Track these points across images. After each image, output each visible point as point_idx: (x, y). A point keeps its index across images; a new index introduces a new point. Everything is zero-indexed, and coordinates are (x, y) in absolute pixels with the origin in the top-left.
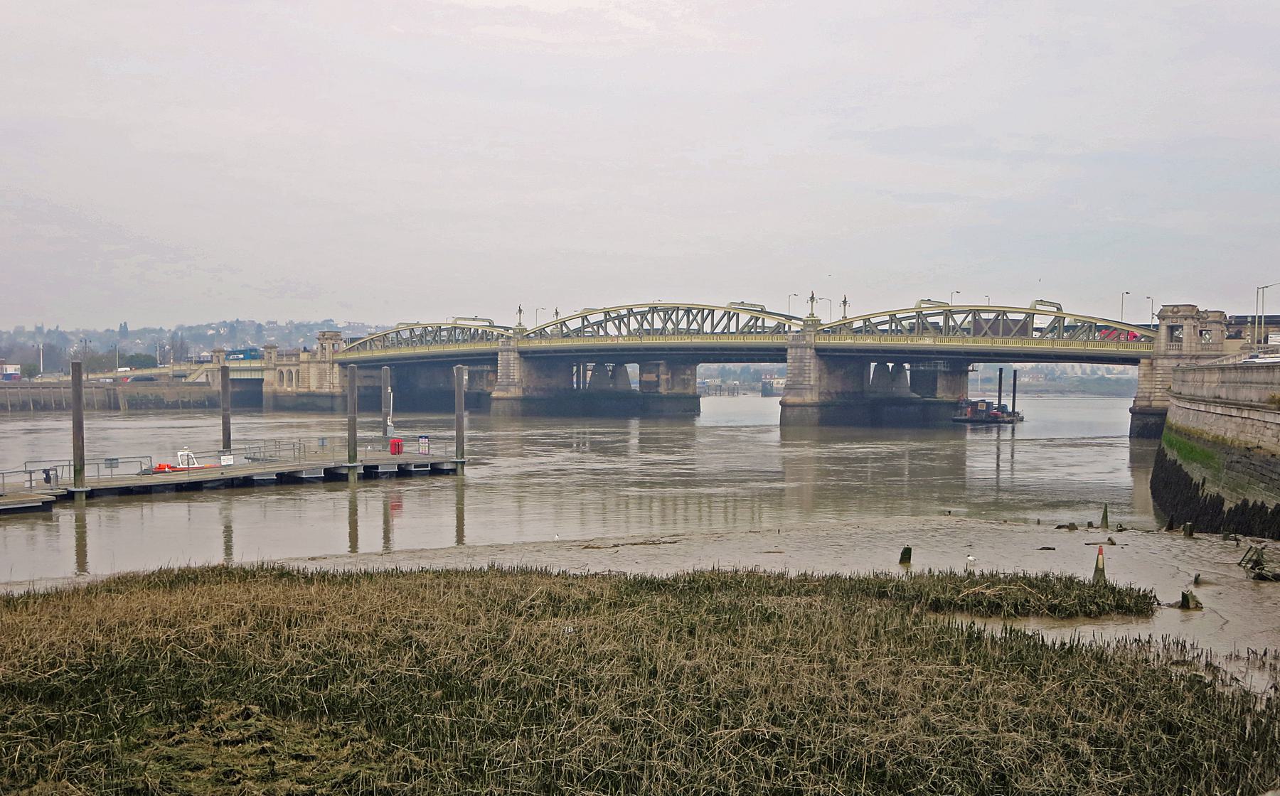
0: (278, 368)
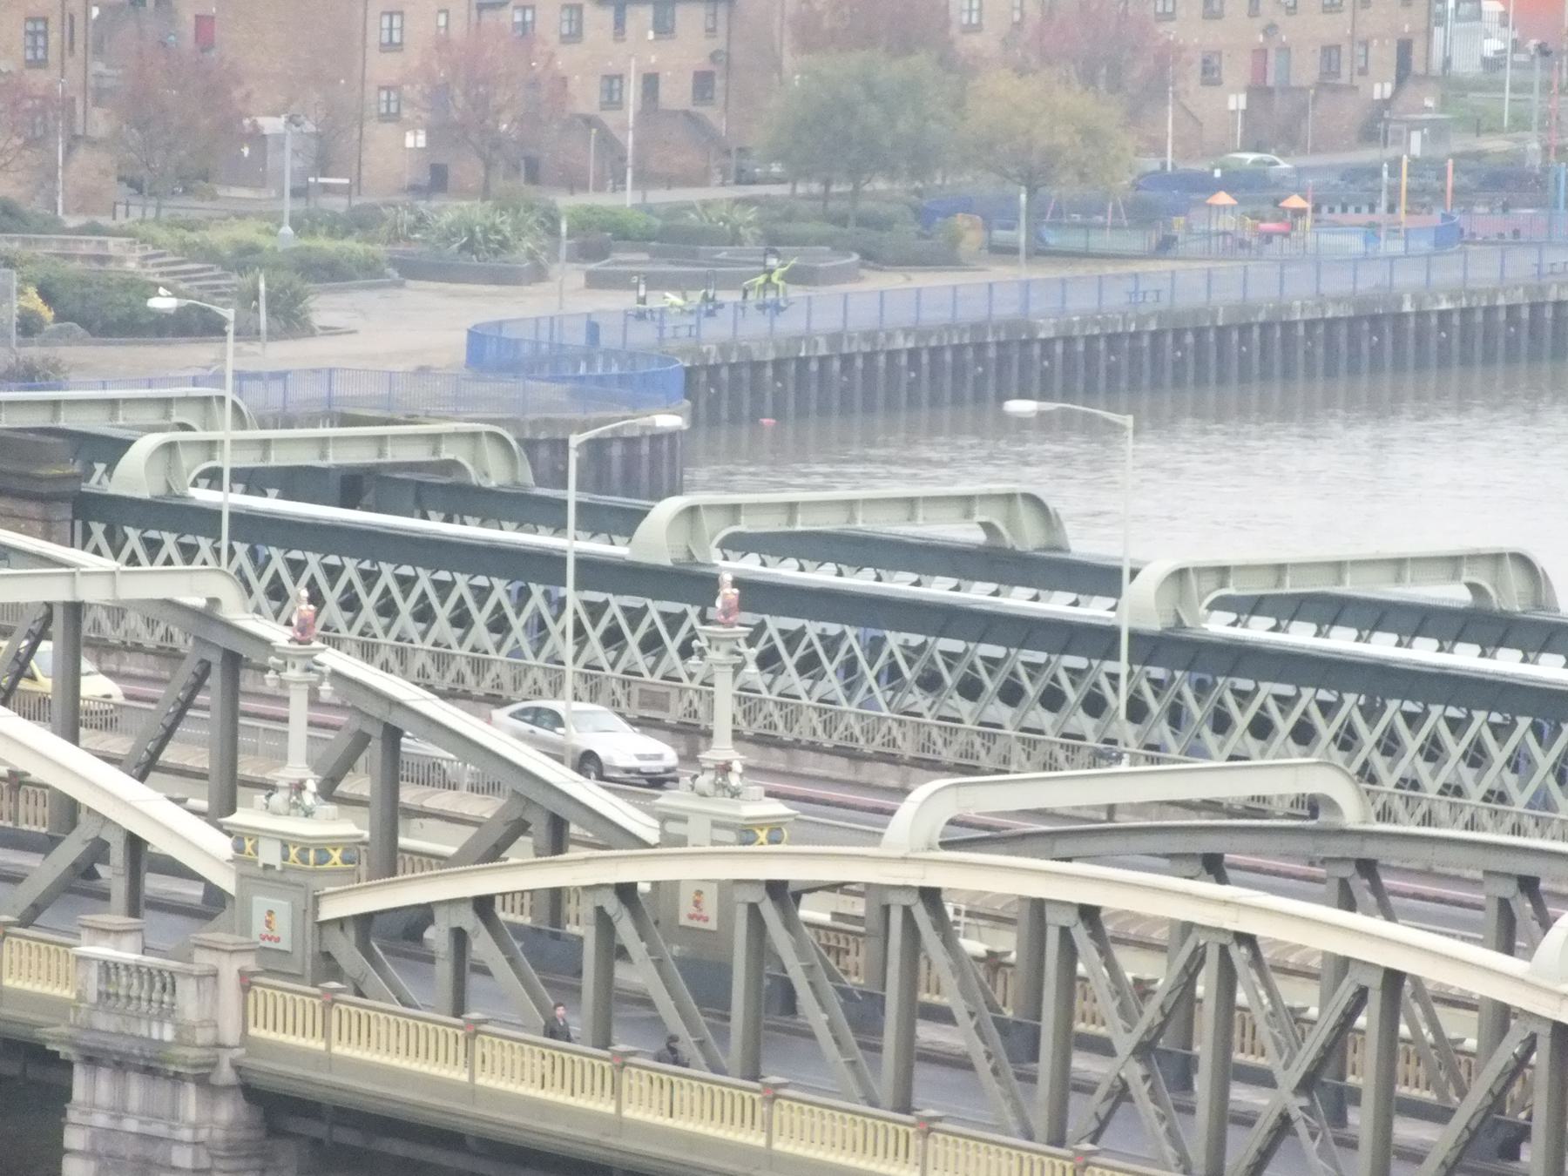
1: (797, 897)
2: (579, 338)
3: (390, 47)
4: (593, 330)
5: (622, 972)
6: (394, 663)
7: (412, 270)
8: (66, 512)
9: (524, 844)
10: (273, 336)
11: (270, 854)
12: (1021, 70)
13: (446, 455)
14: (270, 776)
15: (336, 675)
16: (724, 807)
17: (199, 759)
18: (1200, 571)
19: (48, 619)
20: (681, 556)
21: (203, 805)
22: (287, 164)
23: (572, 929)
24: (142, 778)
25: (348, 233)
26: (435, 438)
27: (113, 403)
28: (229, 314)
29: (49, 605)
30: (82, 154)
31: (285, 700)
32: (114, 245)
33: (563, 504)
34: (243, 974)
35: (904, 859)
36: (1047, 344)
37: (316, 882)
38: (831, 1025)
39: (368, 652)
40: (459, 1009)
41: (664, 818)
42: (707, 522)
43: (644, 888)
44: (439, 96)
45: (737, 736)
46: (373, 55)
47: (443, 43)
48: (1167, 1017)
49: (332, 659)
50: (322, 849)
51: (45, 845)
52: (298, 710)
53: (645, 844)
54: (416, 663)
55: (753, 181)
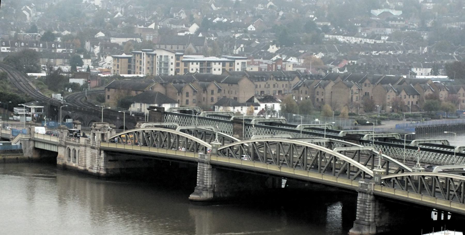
0: (68, 146)
1: (425, 177)
2: (406, 126)
3: (389, 99)
4: (407, 125)
5: (409, 184)
6: (388, 155)
7: (390, 119)
8: (359, 141)
9: (400, 172)
10: (378, 125)
11: (377, 173)
12: (446, 101)
13: (394, 136)
14: (377, 166)
15: (383, 157)
16: (418, 168)
17: (370, 164)
18: (462, 147)
19: (357, 151)
20: (415, 145)
21: (371, 168)
22: (379, 110)
23: (404, 180)
24: (365, 166)
25: (385, 116)
26: (393, 135)
27: (363, 131)
28: (374, 123)
29: (357, 150)
30: (361, 109)
31: (378, 159)
32: (363, 117)
33: (404, 141)
34: (374, 184)
35: (435, 173)
36: (448, 126)
37: (381, 176)
38: (428, 189)
39: (386, 154)
40: (394, 187)
41: (413, 169)
42: (417, 142)
43: (411, 176)
44: (392, 103)
45: (420, 162)
46: (387, 99)
47: (393, 99)
48: (459, 188)
49: (383, 155)
50: (382, 172)
51: (356, 172)
52: (380, 160)
53: (410, 172)
54: (390, 155)
55: (421, 111)
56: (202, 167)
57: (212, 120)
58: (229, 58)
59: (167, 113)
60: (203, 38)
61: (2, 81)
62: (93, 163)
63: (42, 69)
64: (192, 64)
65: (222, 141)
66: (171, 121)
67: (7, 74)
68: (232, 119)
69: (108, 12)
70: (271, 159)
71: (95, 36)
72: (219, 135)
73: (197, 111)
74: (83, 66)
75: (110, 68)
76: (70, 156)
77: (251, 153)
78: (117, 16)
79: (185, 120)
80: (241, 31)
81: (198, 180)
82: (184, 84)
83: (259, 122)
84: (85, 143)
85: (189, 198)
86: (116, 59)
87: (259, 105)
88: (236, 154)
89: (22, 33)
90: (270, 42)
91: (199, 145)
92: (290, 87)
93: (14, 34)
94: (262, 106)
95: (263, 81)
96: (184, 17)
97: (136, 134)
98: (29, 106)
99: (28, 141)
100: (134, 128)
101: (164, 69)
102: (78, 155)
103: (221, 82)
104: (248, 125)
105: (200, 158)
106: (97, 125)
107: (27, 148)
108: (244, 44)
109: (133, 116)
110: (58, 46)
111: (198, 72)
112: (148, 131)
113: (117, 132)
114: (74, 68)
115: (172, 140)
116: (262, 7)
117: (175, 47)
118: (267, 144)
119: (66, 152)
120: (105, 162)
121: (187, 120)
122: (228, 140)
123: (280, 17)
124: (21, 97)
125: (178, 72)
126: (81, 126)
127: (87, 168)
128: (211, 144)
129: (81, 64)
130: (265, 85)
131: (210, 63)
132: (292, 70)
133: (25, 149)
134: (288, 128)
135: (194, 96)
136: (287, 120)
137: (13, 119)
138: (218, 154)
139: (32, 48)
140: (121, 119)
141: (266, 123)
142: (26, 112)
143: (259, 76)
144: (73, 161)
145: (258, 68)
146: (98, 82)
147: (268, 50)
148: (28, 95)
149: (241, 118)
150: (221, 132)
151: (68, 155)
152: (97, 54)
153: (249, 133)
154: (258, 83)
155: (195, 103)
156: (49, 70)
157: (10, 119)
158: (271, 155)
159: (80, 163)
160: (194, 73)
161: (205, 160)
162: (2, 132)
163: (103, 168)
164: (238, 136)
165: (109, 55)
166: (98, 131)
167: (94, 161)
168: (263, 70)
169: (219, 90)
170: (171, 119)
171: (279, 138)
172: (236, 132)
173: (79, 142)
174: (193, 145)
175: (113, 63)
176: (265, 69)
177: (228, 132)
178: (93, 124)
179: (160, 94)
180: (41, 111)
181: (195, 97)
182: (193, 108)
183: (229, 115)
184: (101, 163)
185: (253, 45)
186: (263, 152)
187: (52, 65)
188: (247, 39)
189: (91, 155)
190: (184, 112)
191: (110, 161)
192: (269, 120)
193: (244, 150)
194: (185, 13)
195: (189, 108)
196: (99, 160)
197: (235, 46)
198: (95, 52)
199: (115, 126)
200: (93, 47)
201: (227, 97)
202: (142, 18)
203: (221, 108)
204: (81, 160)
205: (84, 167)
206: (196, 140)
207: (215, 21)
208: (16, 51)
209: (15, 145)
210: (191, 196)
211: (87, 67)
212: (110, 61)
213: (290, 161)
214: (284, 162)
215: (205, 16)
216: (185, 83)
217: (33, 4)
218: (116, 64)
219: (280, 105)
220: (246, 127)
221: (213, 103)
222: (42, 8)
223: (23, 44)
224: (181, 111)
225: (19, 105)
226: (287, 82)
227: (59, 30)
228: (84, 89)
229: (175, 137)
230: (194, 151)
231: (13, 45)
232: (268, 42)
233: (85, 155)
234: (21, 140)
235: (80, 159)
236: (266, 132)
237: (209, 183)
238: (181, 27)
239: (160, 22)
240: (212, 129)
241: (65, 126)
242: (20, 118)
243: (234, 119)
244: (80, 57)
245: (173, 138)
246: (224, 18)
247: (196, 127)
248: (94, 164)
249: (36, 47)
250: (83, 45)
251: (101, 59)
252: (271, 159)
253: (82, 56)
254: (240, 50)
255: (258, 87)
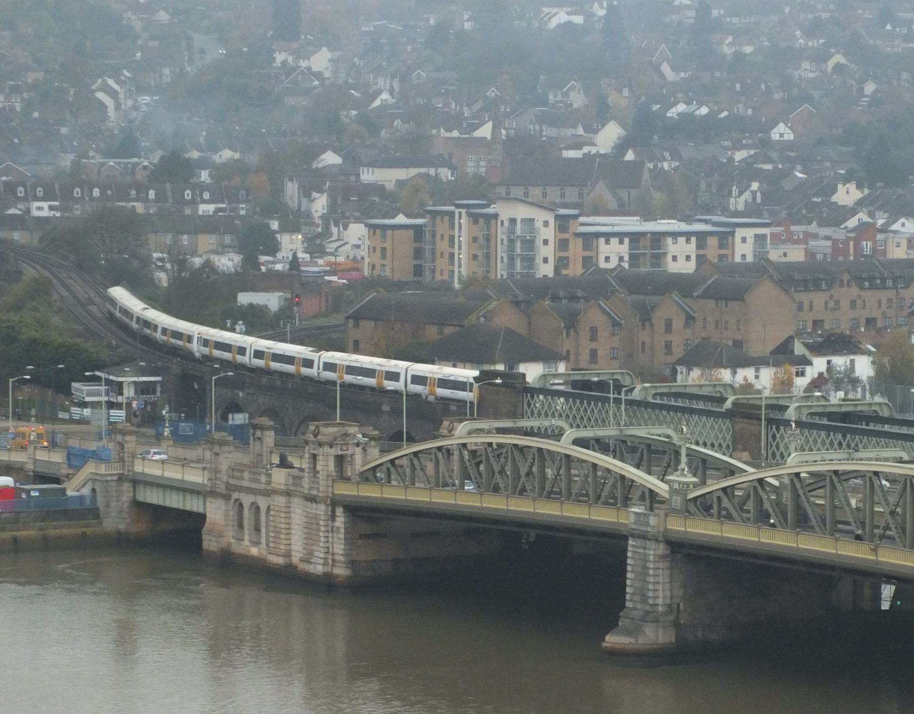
0: (235, 495)
56: (641, 550)
57: (669, 408)
58: (715, 224)
59: (533, 391)
60: (637, 166)
61: (34, 304)
62: (312, 545)
63: (155, 264)
64: (607, 242)
65: (699, 473)
66: (547, 415)
67: (50, 282)
68: (728, 404)
69: (353, 92)
70: (848, 523)
71: (314, 165)
72: (691, 454)
73: (622, 383)
74: (279, 256)
75: (359, 258)
76: (241, 526)
77: (787, 505)
78: (377, 103)
79: (589, 411)
80: (750, 141)
81: (628, 590)
82: (581, 305)
83: (808, 414)
84: (286, 485)
85: (604, 644)
86: (378, 231)
87: (810, 363)
88: (741, 509)
89: (93, 158)
90: (839, 174)
91: (631, 486)
92: (901, 308)
93: (69, 163)
94: (819, 365)
95: (818, 288)
96: (581, 104)
97: (440, 455)
98: (118, 376)
99: (114, 484)
100: (436, 437)
101: (524, 259)
102: (267, 521)
103: (695, 294)
104: (777, 423)
105: (635, 523)
106: (322, 429)
107: (113, 504)
108: (761, 182)
109: (430, 402)
110: (201, 195)
111: (626, 265)
112: (476, 444)
113: (383, 451)
114: (250, 261)
115: (549, 472)
116: (812, 71)
117: (554, 194)
118: (835, 479)
119: (231, 513)
120: (350, 540)
121: (593, 410)
122: (718, 469)
123: (867, 99)
124: (92, 350)
125: (566, 266)
126: (276, 434)
127: (295, 560)
128: (666, 482)
129: (273, 248)
130: (826, 303)
131: (659, 241)
132: (904, 257)
133: (107, 506)
134: (895, 429)
135: (614, 338)
136: (895, 406)
137: (71, 416)
138: (688, 512)
139: (124, 204)
140: (396, 412)
141: (830, 416)
142: (107, 394)
143: (809, 277)
144: (250, 541)
145: (803, 250)
146: (324, 299)
147: (834, 199)
148: (114, 342)
149: (758, 402)
150: (697, 444)
151: (236, 523)
152: (322, 217)
153: (782, 446)
154: (804, 297)
155: (616, 359)
156: (176, 267)
157: (60, 416)
158: (849, 512)
159: (271, 545)
160: (612, 271)
161: (649, 529)
162: (37, 458)
163: (342, 559)
164: (746, 455)
165: (358, 220)
166: (327, 449)
167: (314, 538)
168: (819, 257)
169: (690, 320)
170: (546, 408)
171: (868, 459)
172: (739, 443)
173: (269, 483)
174: (614, 486)
175: (367, 243)
176: (825, 255)
177: (716, 445)
178: (312, 428)
179: (510, 334)
180: (154, 393)
181: (616, 341)
182: (613, 374)
183: (720, 392)
184: (335, 544)
185: (787, 185)
186: (823, 502)
187: (186, 254)
188: (769, 167)
189: (305, 520)
190: (586, 385)
191: (362, 537)
192: (840, 405)
193: (765, 497)
194: (581, 92)
195: (598, 375)
196: (330, 535)
197: (734, 188)
198: (313, 211)
199: (377, 433)
200: (308, 195)
201: (713, 340)
202: (453, 107)
203: (696, 373)
204: (274, 537)
205: (285, 556)
206: (622, 469)
207: (672, 113)
208: (77, 213)
209: (75, 494)
210: (607, 638)
211: (291, 258)
212: (360, 239)
213: (904, 530)
214: (888, 533)
215: (643, 98)
216: (586, 299)
217: (125, 72)
218: (379, 246)
219: (873, 363)
220: (771, 428)
221: (671, 359)
222: (153, 84)
223: (96, 192)
224: (575, 384)
225: (87, 374)
226: (891, 294)
227: (205, 148)
228: (282, 322)
229: (557, 462)
230: (615, 504)
231: (66, 195)
232: (832, 173)
233: (288, 521)
234: (94, 481)
235: (272, 534)
236: (832, 444)
237: (664, 598)
238: (570, 131)
239: (507, 121)
240: (668, 436)
241: (225, 434)
242: (91, 413)
243: (734, 404)
244: (268, 226)
245: (554, 463)
246: (701, 105)
247: (621, 430)
248: (315, 548)
249: (137, 200)
250: (277, 191)
251: (332, 234)
252: (848, 523)
253: (275, 225)
254: (750, 200)
255: (806, 307)
